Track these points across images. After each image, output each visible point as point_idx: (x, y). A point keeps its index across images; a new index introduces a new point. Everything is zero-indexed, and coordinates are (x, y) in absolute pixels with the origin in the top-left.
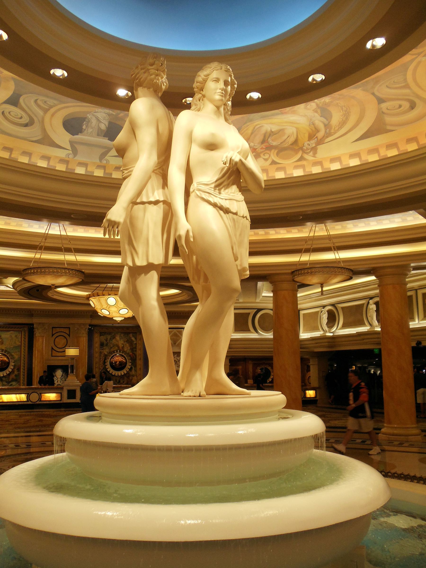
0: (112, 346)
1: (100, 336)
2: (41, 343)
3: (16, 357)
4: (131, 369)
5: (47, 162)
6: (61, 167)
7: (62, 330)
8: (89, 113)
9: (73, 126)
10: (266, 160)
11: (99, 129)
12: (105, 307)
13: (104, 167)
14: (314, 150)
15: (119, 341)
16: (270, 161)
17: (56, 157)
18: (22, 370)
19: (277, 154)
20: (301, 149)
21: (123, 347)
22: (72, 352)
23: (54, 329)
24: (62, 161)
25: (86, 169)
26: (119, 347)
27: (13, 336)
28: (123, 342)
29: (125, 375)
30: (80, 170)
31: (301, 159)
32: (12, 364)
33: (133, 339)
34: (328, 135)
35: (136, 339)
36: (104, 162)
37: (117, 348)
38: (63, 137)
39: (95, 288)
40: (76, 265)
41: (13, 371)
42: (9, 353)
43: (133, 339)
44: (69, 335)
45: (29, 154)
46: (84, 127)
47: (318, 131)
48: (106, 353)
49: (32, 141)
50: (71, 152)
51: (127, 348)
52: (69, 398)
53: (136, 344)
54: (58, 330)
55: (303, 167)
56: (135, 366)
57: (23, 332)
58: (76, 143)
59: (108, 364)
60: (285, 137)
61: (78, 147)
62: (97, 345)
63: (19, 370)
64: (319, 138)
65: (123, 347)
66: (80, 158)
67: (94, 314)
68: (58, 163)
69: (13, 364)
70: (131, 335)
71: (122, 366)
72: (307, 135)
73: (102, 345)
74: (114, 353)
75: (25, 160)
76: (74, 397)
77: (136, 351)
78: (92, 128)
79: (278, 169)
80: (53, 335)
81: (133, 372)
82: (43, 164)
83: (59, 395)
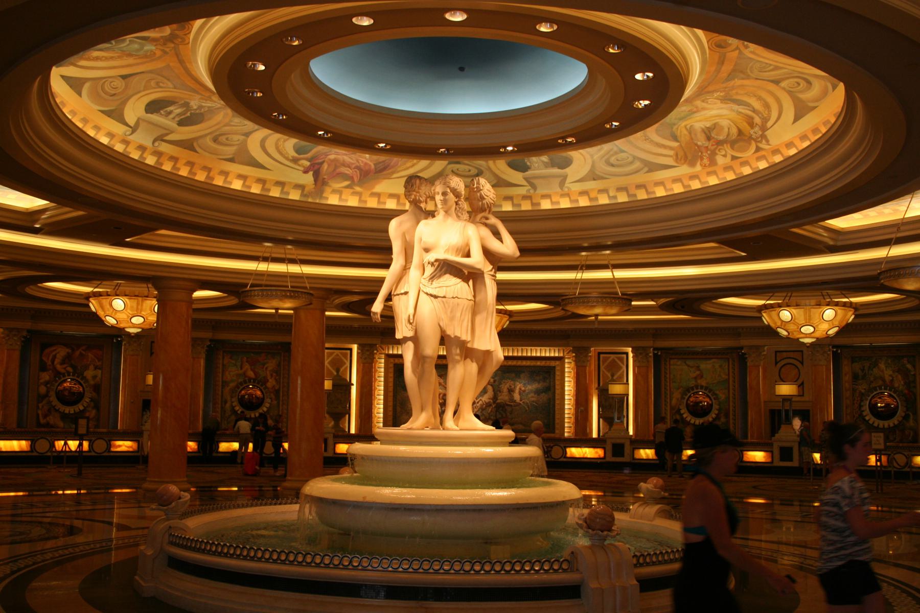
0: (872, 379)
1: (853, 362)
2: (758, 377)
4: (906, 417)
7: (791, 355)
10: (725, 156)
12: (779, 324)
13: (568, 195)
14: (763, 136)
15: (885, 370)
16: (729, 158)
18: (731, 416)
19: (732, 148)
20: (750, 138)
21: (892, 380)
22: (785, 389)
23: (778, 354)
24: (525, 197)
26: (883, 380)
28: (891, 373)
29: (895, 426)
30: (546, 205)
31: (758, 149)
32: (715, 406)
33: (909, 366)
34: (765, 120)
35: (914, 367)
36: (566, 190)
37: (880, 382)
42: (710, 391)
43: (909, 366)
44: (802, 363)
47: (752, 118)
48: (863, 391)
51: (899, 383)
52: (782, 459)
53: (914, 375)
54: (785, 355)
55: (763, 157)
56: (915, 414)
59: (866, 408)
60: (726, 130)
61: (535, 181)
62: (847, 378)
63: (727, 415)
64: (760, 124)
65: (892, 380)
66: (540, 191)
67: (770, 332)
69: (717, 407)
70: (905, 361)
71: (888, 413)
72: (745, 124)
73: (855, 377)
74: (876, 390)
76: (790, 459)
77: (915, 387)
79: (745, 163)
80: (776, 363)
81: (911, 423)
83: (770, 454)
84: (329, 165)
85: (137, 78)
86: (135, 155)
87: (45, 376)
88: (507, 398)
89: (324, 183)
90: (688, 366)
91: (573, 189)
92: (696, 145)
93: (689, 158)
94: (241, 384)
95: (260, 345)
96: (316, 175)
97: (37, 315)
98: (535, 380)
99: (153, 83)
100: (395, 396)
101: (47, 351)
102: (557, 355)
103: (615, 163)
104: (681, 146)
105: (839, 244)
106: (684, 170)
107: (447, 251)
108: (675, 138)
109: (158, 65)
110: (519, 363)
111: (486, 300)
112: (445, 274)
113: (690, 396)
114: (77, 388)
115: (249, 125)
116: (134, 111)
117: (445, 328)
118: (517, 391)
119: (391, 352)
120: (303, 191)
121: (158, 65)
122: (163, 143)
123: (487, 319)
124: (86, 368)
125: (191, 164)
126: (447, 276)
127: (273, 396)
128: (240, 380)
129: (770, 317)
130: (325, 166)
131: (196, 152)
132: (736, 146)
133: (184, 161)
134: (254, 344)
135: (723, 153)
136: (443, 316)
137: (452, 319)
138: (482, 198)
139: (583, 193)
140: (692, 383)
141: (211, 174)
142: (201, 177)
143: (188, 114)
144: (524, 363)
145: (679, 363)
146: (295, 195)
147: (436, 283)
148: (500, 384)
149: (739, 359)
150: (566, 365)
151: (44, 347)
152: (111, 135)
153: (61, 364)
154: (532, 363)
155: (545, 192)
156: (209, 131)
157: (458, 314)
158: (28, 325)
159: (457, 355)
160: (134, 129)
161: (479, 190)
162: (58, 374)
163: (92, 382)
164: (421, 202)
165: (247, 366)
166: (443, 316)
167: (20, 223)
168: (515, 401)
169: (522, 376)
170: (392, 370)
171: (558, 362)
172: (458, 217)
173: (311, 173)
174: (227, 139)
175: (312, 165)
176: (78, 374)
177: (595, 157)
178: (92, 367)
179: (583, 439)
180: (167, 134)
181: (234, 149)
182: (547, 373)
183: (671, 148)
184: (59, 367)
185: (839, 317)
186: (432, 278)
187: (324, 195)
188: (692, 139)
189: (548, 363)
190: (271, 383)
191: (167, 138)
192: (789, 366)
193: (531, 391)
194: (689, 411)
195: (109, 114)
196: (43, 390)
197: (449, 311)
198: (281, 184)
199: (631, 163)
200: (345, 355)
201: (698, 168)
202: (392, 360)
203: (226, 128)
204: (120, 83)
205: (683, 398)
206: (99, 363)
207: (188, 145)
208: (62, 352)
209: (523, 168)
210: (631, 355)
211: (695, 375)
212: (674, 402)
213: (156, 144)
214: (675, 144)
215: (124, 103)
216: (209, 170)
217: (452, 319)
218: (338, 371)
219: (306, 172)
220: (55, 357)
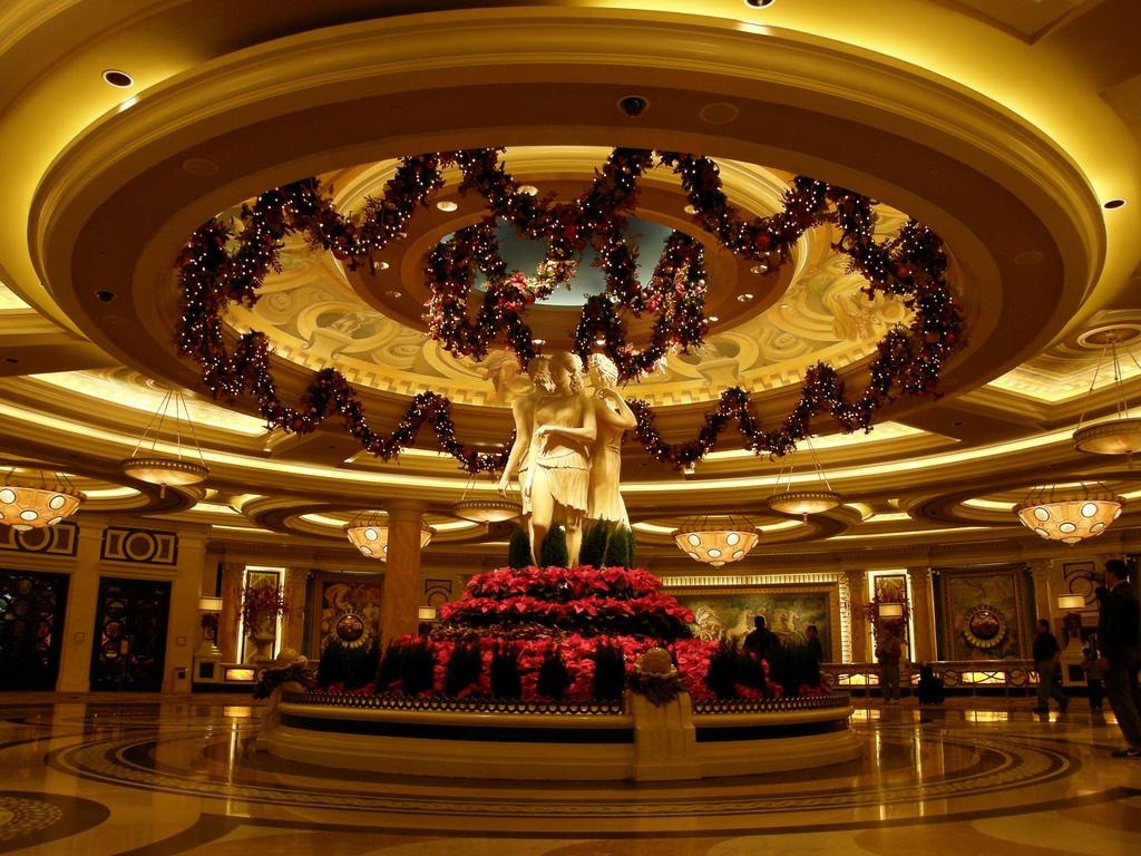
2: (1043, 589)
3: (1009, 616)
10: (880, 324)
19: (884, 314)
24: (702, 390)
27: (1001, 583)
40: (819, 485)
41: (1005, 639)
42: (995, 610)
57: (1015, 578)
58: (706, 369)
61: (709, 373)
63: (1015, 636)
69: (1004, 627)
80: (1066, 577)
84: (507, 371)
87: (328, 613)
88: (780, 627)
89: (506, 390)
90: (970, 585)
91: (747, 377)
92: (850, 316)
93: (849, 331)
96: (496, 381)
97: (319, 554)
98: (808, 608)
99: (316, 297)
101: (329, 589)
102: (830, 580)
103: (782, 345)
104: (836, 319)
105: (1052, 419)
106: (845, 345)
108: (828, 312)
109: (314, 278)
110: (792, 590)
113: (973, 618)
114: (358, 626)
116: (307, 325)
118: (791, 620)
120: (485, 397)
121: (314, 278)
122: (343, 357)
124: (365, 605)
125: (372, 375)
126: (559, 447)
129: (1027, 518)
130: (503, 373)
132: (887, 312)
135: (878, 321)
136: (556, 487)
137: (565, 488)
138: (601, 373)
140: (976, 603)
142: (383, 387)
143: (359, 326)
144: (797, 590)
145: (960, 582)
146: (478, 402)
148: (773, 613)
149: (1024, 576)
150: (841, 591)
151: (326, 585)
153: (342, 602)
154: (806, 590)
156: (386, 341)
158: (310, 564)
160: (311, 343)
161: (597, 365)
162: (339, 611)
163: (370, 619)
164: (544, 382)
167: (251, 448)
168: (789, 631)
169: (795, 603)
171: (832, 588)
173: (491, 380)
174: (403, 350)
175: (491, 372)
176: (358, 610)
178: (370, 605)
179: (861, 667)
180: (344, 347)
181: (412, 359)
182: (820, 599)
183: (829, 324)
184: (340, 605)
185: (1101, 513)
186: (545, 451)
187: (507, 401)
188: (844, 310)
189: (822, 589)
192: (1077, 581)
193: (806, 619)
194: (973, 632)
196: (326, 626)
197: (561, 482)
198: (463, 392)
199: (796, 343)
201: (859, 341)
204: (284, 298)
205: (965, 619)
206: (376, 601)
207: (366, 357)
208: (343, 590)
209: (696, 361)
210: (908, 576)
211: (977, 594)
212: (957, 624)
213: (335, 357)
214: (833, 318)
217: (565, 488)
219: (485, 379)
220: (336, 595)
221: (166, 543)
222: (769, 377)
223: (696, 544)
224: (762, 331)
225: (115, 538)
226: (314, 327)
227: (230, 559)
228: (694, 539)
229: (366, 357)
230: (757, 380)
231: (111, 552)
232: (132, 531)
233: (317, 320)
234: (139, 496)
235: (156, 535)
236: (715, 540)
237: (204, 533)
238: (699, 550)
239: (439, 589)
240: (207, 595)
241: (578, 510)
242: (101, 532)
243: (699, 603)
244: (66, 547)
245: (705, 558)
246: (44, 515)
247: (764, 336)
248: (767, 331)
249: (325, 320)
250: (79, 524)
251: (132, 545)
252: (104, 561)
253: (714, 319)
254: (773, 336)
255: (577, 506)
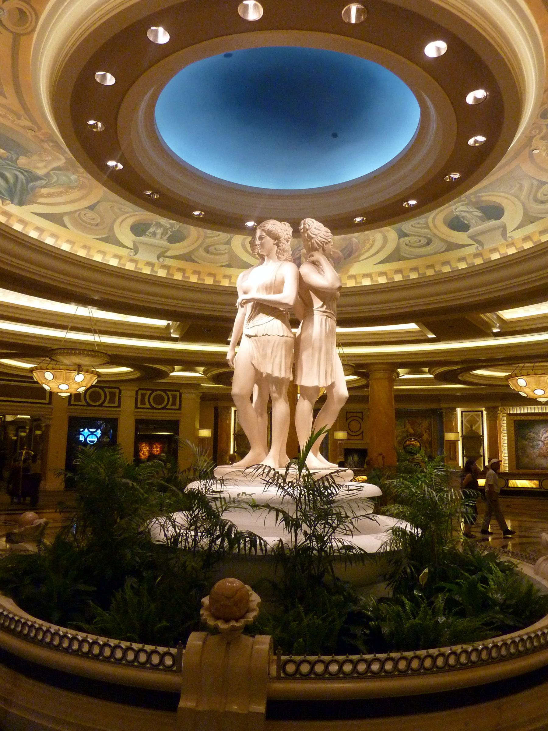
5: (449, 266)
6: (478, 261)
8: (452, 211)
9: (458, 224)
11: (477, 216)
17: (469, 255)
24: (476, 255)
25: (500, 253)
30: (495, 256)
36: (510, 239)
38: (460, 237)
39: (515, 368)
45: (447, 263)
46: (466, 222)
49: (442, 252)
50: (477, 245)
61: (480, 238)
66: (488, 247)
68: (474, 258)
75: (447, 269)
78: (472, 219)
82: (463, 266)
85: (101, 208)
86: (147, 271)
94: (405, 438)
95: (416, 411)
100: (516, 444)
103: (544, 198)
107: (258, 290)
111: (311, 337)
112: (259, 313)
115: (223, 236)
117: (257, 367)
119: (511, 412)
123: (313, 355)
127: (427, 446)
128: (405, 435)
131: (197, 262)
133: (191, 271)
134: (411, 411)
137: (264, 356)
138: (310, 238)
139: (527, 238)
141: (217, 279)
142: (209, 281)
143: (170, 233)
147: (253, 323)
152: (119, 257)
155: (492, 246)
157: (269, 352)
159: (274, 392)
161: (306, 230)
165: (408, 426)
166: (256, 355)
167: (158, 335)
170: (513, 425)
172: (279, 258)
174: (215, 249)
177: (522, 198)
180: (166, 252)
190: (425, 437)
191: (166, 254)
195: (106, 240)
197: (261, 350)
200: (478, 416)
202: (512, 417)
203: (208, 240)
204: (90, 214)
207: (187, 257)
213: (161, 260)
215: (111, 229)
216: (214, 276)
218: (471, 427)
221: (174, 397)
222: (538, 235)
223: (522, 384)
224: (521, 188)
225: (143, 395)
226: (133, 237)
227: (221, 404)
228: (522, 382)
229: (187, 257)
230: (527, 238)
231: (141, 404)
232: (154, 391)
233: (131, 230)
234: (132, 372)
235: (168, 393)
236: (539, 381)
237: (197, 390)
238: (527, 390)
239: (357, 418)
240: (202, 426)
241: (277, 378)
242: (134, 393)
243: (542, 426)
244: (114, 403)
245: (531, 395)
246: (73, 386)
247: (525, 190)
248: (526, 184)
249: (139, 229)
250: (121, 388)
251: (154, 399)
252: (137, 410)
253: (456, 176)
254: (534, 189)
255: (276, 374)
